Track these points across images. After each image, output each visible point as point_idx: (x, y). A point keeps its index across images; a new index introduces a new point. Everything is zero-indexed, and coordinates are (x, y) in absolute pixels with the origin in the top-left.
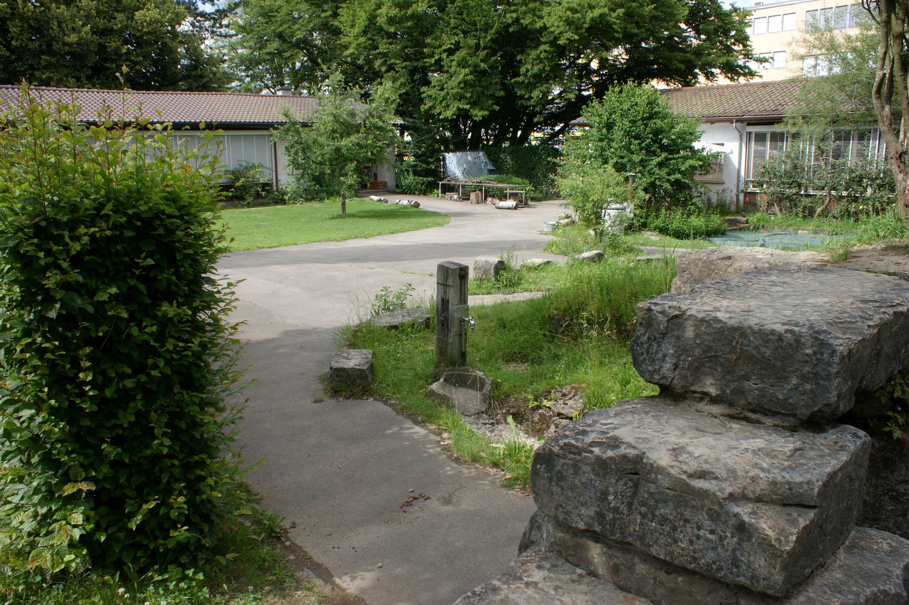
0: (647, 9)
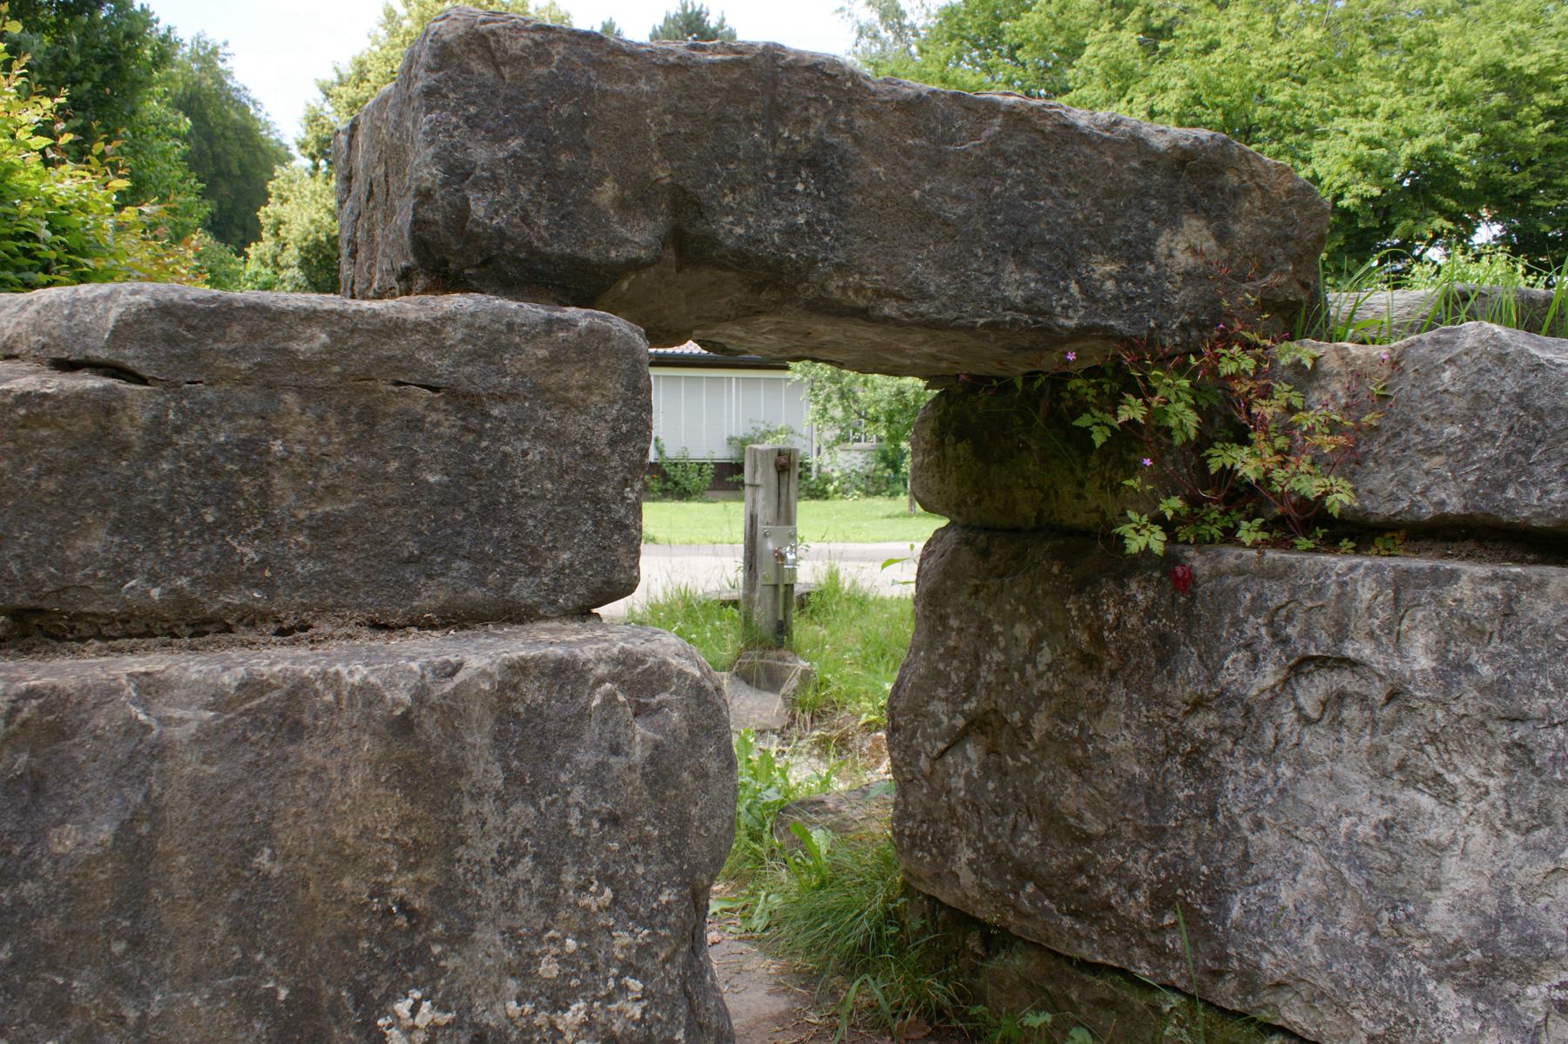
0: (1534, 132)
